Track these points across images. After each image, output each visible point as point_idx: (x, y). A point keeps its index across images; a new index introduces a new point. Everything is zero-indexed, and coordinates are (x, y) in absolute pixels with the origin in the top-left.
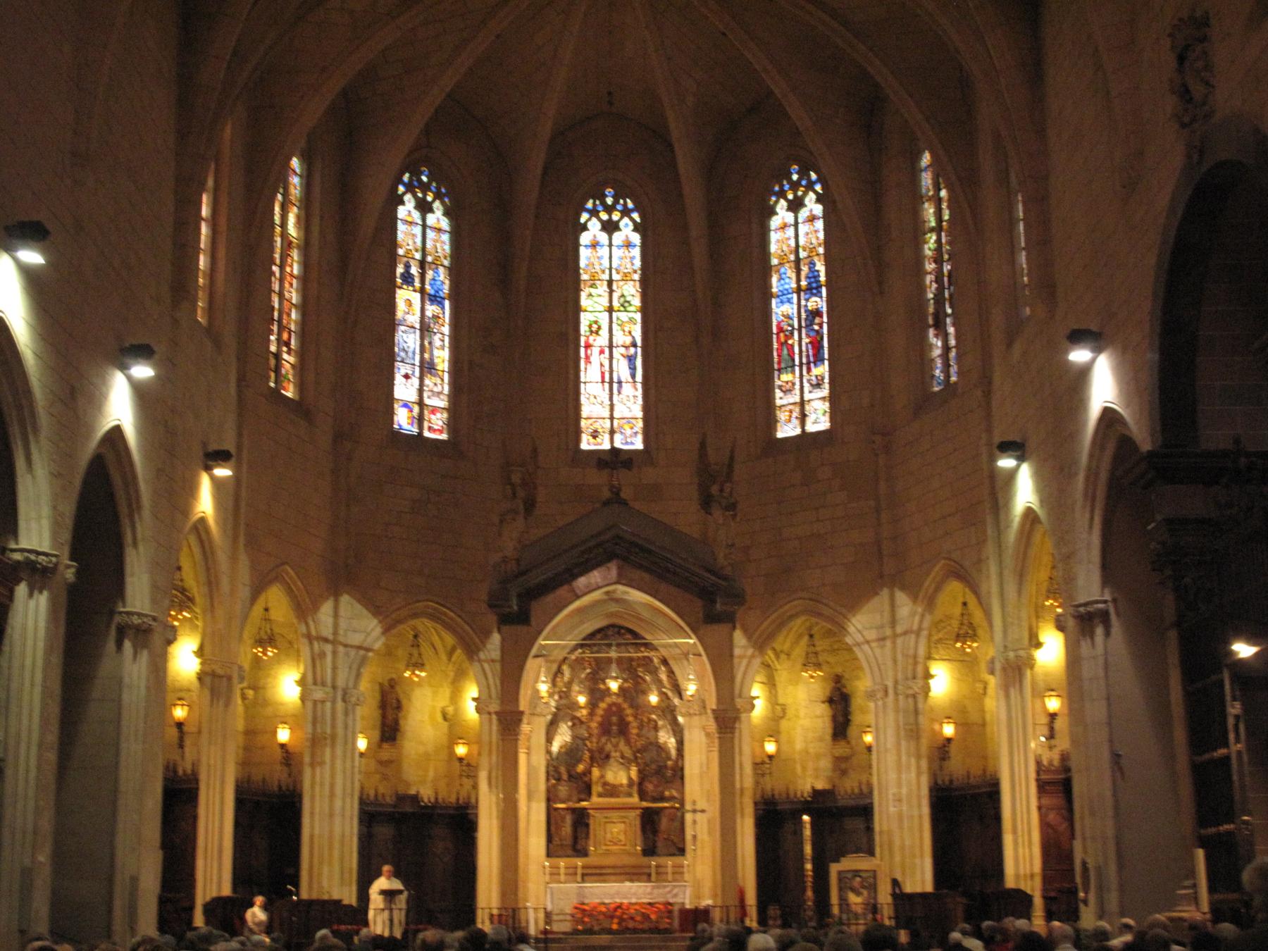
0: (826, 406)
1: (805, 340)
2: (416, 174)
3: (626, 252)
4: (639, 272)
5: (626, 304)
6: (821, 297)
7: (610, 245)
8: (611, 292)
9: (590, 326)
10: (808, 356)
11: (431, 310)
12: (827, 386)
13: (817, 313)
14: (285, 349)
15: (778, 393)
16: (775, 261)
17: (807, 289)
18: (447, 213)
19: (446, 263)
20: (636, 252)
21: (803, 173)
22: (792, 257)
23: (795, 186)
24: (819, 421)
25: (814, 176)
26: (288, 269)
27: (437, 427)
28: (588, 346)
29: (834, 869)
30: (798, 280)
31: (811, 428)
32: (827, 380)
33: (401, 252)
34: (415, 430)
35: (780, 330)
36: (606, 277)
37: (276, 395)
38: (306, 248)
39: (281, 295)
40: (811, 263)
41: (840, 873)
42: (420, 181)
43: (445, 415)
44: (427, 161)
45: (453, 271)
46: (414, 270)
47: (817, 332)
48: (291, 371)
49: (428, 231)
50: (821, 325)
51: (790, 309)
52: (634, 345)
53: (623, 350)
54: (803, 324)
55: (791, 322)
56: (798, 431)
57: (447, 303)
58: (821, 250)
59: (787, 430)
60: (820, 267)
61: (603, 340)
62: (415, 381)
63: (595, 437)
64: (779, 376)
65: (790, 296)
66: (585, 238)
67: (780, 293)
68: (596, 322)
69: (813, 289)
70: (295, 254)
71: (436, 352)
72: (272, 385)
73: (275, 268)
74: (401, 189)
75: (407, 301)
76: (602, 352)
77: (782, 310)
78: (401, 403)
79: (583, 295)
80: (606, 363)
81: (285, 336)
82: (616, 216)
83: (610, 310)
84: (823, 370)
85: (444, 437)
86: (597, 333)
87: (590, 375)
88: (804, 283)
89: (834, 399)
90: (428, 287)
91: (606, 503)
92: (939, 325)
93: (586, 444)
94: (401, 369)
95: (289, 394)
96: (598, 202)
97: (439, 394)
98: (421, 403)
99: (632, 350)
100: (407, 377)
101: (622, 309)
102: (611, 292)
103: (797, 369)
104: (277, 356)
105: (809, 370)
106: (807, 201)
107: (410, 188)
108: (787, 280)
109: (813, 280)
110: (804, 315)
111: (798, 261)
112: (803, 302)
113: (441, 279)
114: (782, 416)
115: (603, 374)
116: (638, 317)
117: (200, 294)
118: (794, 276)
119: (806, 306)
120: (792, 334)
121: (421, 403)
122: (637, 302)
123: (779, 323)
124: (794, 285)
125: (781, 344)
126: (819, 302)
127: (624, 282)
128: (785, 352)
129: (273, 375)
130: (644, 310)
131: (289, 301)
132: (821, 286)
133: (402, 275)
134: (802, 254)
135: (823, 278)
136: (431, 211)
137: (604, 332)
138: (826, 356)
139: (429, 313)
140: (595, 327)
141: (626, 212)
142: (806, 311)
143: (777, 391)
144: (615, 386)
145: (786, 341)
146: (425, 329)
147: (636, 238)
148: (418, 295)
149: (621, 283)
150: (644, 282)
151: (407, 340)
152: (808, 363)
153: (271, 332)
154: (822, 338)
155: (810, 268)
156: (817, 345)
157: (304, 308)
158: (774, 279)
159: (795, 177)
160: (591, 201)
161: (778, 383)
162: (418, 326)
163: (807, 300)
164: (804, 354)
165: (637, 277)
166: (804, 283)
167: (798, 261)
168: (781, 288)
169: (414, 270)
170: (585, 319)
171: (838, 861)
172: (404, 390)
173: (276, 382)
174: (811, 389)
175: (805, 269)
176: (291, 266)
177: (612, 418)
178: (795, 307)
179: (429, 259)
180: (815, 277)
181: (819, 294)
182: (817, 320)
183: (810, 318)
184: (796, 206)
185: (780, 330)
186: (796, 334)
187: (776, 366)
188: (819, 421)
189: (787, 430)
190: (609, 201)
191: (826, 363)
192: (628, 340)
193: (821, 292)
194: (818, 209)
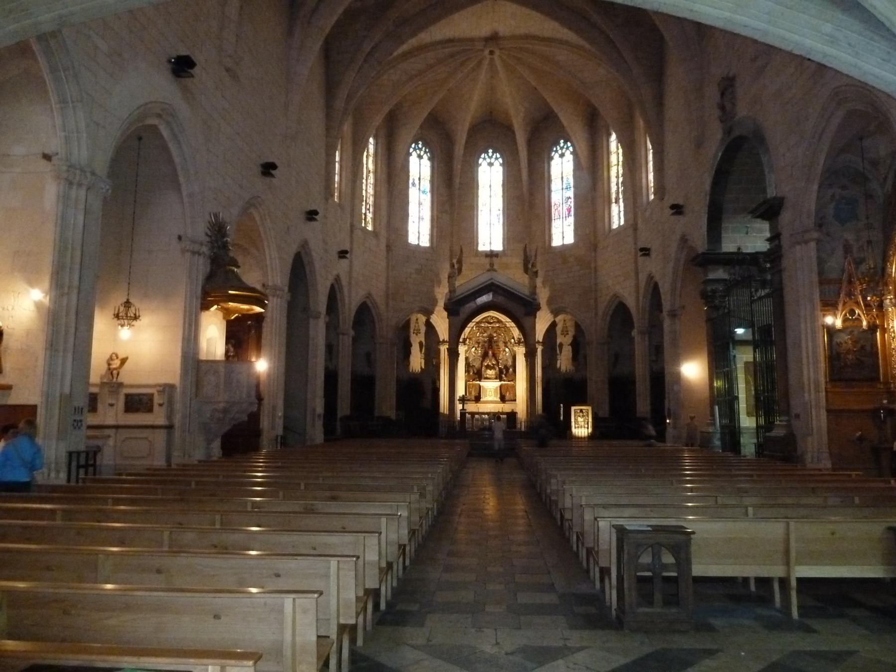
1: (565, 208)
2: (417, 144)
11: (423, 196)
18: (429, 159)
21: (565, 143)
23: (562, 148)
24: (570, 239)
25: (569, 144)
27: (425, 242)
35: (555, 204)
38: (375, 172)
41: (575, 410)
42: (418, 147)
44: (420, 139)
45: (432, 182)
46: (417, 182)
48: (370, 220)
52: (499, 210)
55: (559, 201)
59: (556, 242)
63: (484, 245)
74: (411, 150)
81: (368, 207)
82: (493, 160)
91: (489, 271)
92: (617, 201)
96: (486, 155)
99: (498, 212)
103: (561, 219)
106: (566, 154)
107: (415, 149)
113: (426, 185)
136: (422, 158)
141: (497, 159)
153: (362, 205)
159: (562, 145)
160: (483, 154)
183: (567, 199)
184: (562, 156)
185: (555, 204)
188: (570, 239)
189: (556, 242)
190: (490, 154)
194: (571, 157)
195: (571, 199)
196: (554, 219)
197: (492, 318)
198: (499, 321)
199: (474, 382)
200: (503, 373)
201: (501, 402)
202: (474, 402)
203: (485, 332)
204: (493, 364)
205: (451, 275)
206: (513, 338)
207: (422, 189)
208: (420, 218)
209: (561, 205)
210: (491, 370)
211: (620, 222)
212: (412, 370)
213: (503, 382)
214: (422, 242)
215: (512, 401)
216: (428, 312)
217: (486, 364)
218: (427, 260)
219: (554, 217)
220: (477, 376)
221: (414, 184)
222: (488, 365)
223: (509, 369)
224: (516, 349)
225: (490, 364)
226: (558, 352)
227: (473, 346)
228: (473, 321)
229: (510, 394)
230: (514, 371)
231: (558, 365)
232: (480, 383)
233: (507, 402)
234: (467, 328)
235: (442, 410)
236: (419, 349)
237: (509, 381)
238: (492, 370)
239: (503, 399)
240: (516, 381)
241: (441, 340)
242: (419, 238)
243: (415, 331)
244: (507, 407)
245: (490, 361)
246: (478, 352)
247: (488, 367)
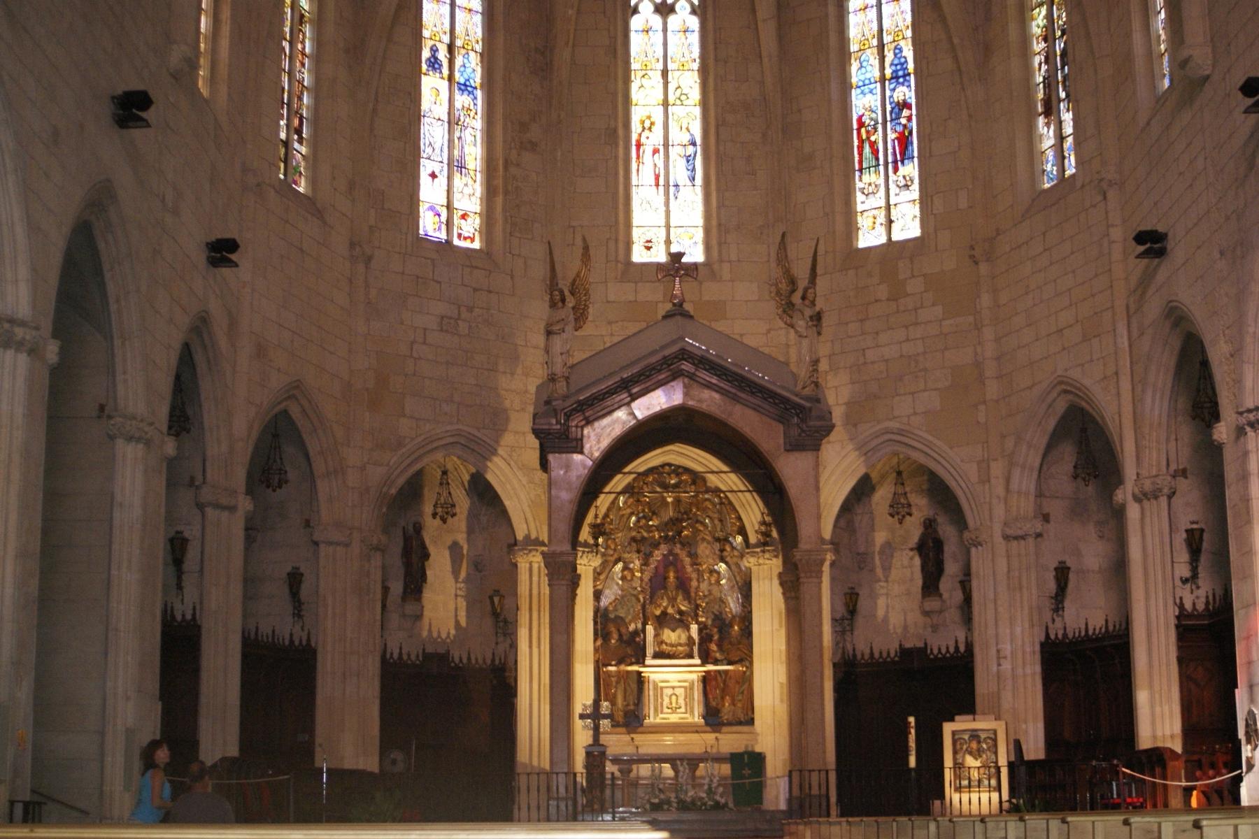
0: (916, 210)
1: (891, 136)
3: (683, 37)
4: (698, 60)
5: (683, 97)
6: (909, 86)
7: (665, 30)
8: (666, 84)
9: (643, 122)
10: (894, 154)
11: (462, 100)
12: (916, 186)
13: (906, 105)
14: (296, 137)
15: (860, 197)
16: (854, 47)
17: (892, 78)
19: (479, 48)
20: (695, 39)
22: (875, 42)
24: (908, 226)
26: (300, 46)
27: (469, 234)
28: (639, 145)
29: (948, 728)
30: (882, 68)
31: (896, 236)
32: (916, 181)
33: (426, 33)
34: (443, 235)
35: (861, 124)
36: (660, 66)
37: (286, 188)
39: (290, 74)
40: (896, 48)
43: (478, 221)
45: (488, 58)
46: (442, 55)
47: (905, 126)
49: (457, 10)
50: (909, 119)
51: (874, 101)
52: (694, 144)
53: (680, 150)
54: (889, 118)
55: (874, 115)
56: (883, 240)
57: (479, 93)
58: (909, 33)
59: (869, 237)
60: (908, 53)
61: (655, 138)
62: (442, 180)
63: (648, 248)
64: (860, 177)
65: (872, 86)
66: (636, 23)
67: (861, 84)
68: (649, 117)
69: (899, 77)
70: (307, 29)
71: (467, 149)
72: (282, 176)
73: (286, 45)
75: (432, 88)
76: (656, 151)
77: (864, 103)
78: (427, 205)
79: (634, 87)
80: (661, 164)
83: (666, 104)
84: (911, 169)
85: (476, 245)
86: (650, 129)
87: (642, 177)
88: (888, 72)
89: (926, 201)
90: (457, 75)
93: (639, 255)
94: (426, 167)
95: (301, 190)
97: (470, 196)
98: (449, 207)
99: (690, 150)
100: (433, 176)
101: (678, 102)
102: (666, 84)
103: (881, 168)
104: (286, 144)
105: (896, 170)
108: (869, 68)
109: (899, 67)
110: (889, 108)
111: (881, 47)
112: (888, 93)
113: (471, 67)
114: (863, 222)
115: (657, 177)
116: (697, 111)
117: (202, 61)
118: (876, 63)
119: (891, 97)
120: (875, 129)
121: (449, 207)
122: (695, 94)
123: (860, 118)
124: (877, 74)
125: (861, 142)
126: (906, 92)
127: (680, 72)
128: (867, 149)
129: (282, 165)
130: (704, 103)
131: (301, 82)
132: (909, 74)
133: (428, 60)
134: (887, 39)
135: (911, 67)
137: (658, 130)
138: (916, 154)
139: (458, 105)
140: (647, 124)
142: (891, 103)
143: (859, 194)
144: (672, 189)
145: (868, 138)
146: (453, 122)
147: (694, 22)
148: (446, 83)
149: (677, 74)
150: (704, 71)
151: (433, 133)
152: (895, 162)
154: (911, 133)
155: (895, 55)
156: (904, 141)
157: (316, 90)
158: (855, 66)
161: (859, 185)
162: (445, 118)
163: (894, 90)
164: (890, 151)
165: (696, 66)
166: (888, 72)
167: (881, 47)
168: (862, 78)
169: (442, 55)
170: (637, 115)
171: (952, 720)
172: (431, 192)
173: (285, 175)
174: (897, 190)
175: (889, 56)
176: (303, 42)
177: (668, 227)
178: (879, 97)
179: (459, 43)
180: (902, 64)
181: (906, 82)
182: (905, 113)
183: (896, 110)
186: (880, 127)
187: (857, 167)
188: (908, 226)
189: (869, 237)
191: (916, 160)
192: (686, 138)
193: (909, 81)
195: (909, 106)
196: (861, 170)
197: (679, 470)
198: (697, 478)
199: (623, 667)
200: (711, 641)
201: (708, 729)
202: (623, 730)
203: (654, 513)
204: (681, 613)
205: (555, 328)
206: (742, 531)
207: (458, 77)
208: (456, 165)
209: (880, 127)
210: (673, 631)
211: (1062, 169)
212: (430, 631)
213: (711, 667)
214: (459, 236)
215: (740, 723)
216: (481, 450)
217: (658, 612)
218: (475, 290)
219: (861, 162)
220: (629, 651)
221: (434, 63)
222: (664, 613)
223: (731, 626)
224: (749, 562)
225: (670, 610)
226: (879, 571)
227: (616, 556)
228: (627, 469)
229: (733, 703)
230: (747, 632)
231: (880, 613)
232: (641, 669)
233: (725, 729)
234: (602, 496)
235: (522, 755)
236: (448, 567)
237: (729, 664)
238: (679, 631)
239: (713, 718)
240: (751, 663)
241: (520, 536)
242: (449, 224)
243: (439, 510)
244: (730, 741)
245: (673, 601)
246: (633, 575)
247: (662, 621)
